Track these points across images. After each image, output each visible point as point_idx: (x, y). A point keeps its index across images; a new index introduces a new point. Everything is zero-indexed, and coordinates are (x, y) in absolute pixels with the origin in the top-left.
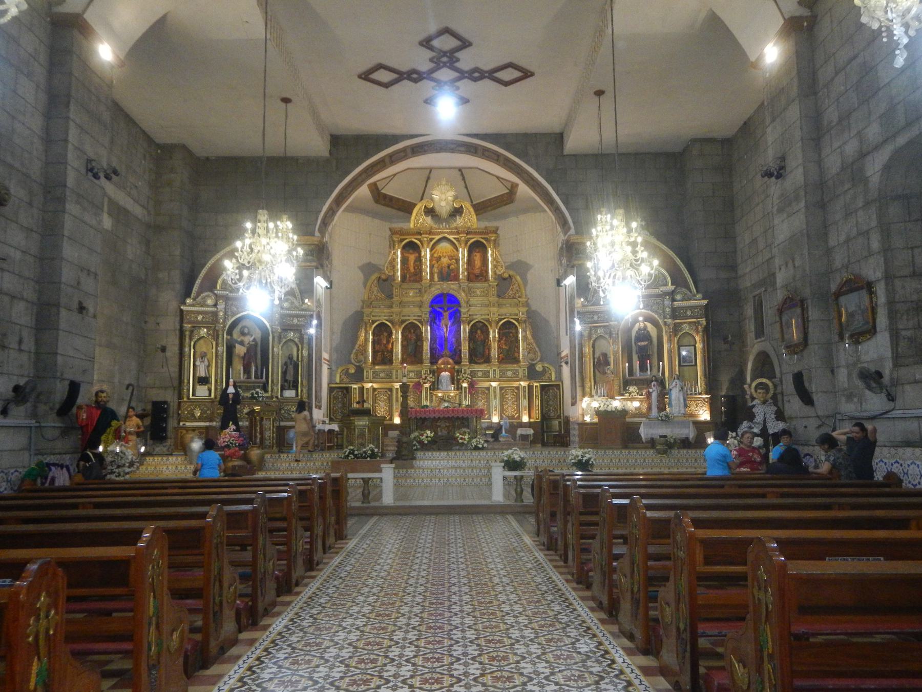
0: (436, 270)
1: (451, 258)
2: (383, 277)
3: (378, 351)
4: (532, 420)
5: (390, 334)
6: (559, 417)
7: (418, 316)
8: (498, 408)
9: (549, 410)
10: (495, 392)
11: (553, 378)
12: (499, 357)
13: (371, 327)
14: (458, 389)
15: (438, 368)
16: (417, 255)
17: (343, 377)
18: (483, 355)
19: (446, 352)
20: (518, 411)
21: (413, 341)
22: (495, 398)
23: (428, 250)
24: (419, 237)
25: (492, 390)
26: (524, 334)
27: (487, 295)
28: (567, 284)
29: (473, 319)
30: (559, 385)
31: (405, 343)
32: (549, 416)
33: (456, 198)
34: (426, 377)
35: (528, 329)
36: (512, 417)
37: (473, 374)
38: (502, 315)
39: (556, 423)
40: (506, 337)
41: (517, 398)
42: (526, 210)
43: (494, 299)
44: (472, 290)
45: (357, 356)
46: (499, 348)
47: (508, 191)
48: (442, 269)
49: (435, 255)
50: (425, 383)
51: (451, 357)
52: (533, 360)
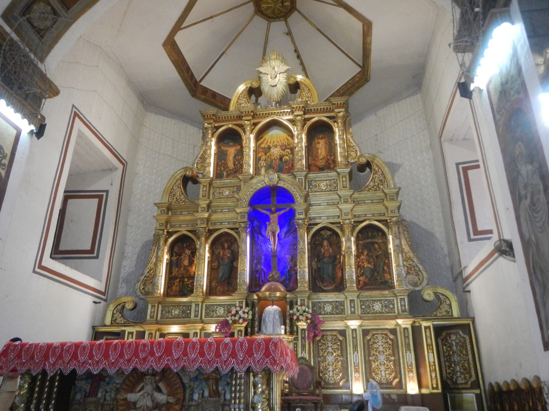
0: (262, 163)
1: (284, 147)
2: (189, 173)
3: (175, 278)
4: (424, 391)
5: (193, 253)
6: (476, 385)
7: (235, 223)
8: (362, 367)
9: (454, 372)
10: (355, 338)
11: (456, 313)
12: (358, 282)
13: (166, 241)
14: (292, 333)
15: (259, 299)
16: (239, 147)
17: (118, 315)
18: (333, 278)
19: (275, 273)
20: (398, 373)
21: (226, 261)
22: (355, 348)
23: (252, 136)
24: (240, 122)
25: (349, 334)
26: (397, 242)
27: (335, 190)
28: (484, 88)
29: (316, 224)
30: (469, 325)
31: (215, 264)
32: (455, 383)
33: (289, 73)
34: (237, 312)
35: (402, 236)
36: (388, 385)
37: (317, 309)
38: (359, 216)
39: (469, 396)
40: (370, 251)
41: (394, 347)
42: (386, 102)
43: (345, 193)
44: (314, 183)
45: (145, 284)
46: (358, 266)
47: (360, 69)
48: (272, 161)
49: (263, 146)
50: (235, 322)
51: (282, 283)
52: (415, 285)
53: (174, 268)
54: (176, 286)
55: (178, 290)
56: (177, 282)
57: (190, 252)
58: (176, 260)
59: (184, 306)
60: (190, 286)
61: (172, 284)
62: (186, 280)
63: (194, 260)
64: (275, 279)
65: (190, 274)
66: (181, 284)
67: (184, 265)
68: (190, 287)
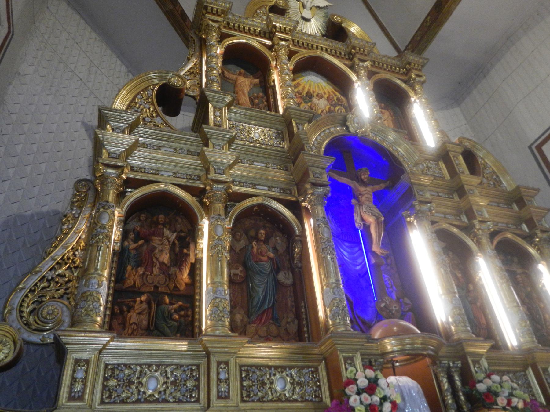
3: (135, 292)
13: (121, 195)
53: (129, 268)
54: (140, 313)
55: (145, 323)
56: (141, 302)
57: (175, 234)
58: (135, 249)
59: (179, 366)
60: (176, 316)
61: (125, 309)
62: (167, 300)
63: (189, 255)
64: (393, 314)
65: (176, 287)
66: (154, 306)
67: (162, 264)
68: (175, 320)
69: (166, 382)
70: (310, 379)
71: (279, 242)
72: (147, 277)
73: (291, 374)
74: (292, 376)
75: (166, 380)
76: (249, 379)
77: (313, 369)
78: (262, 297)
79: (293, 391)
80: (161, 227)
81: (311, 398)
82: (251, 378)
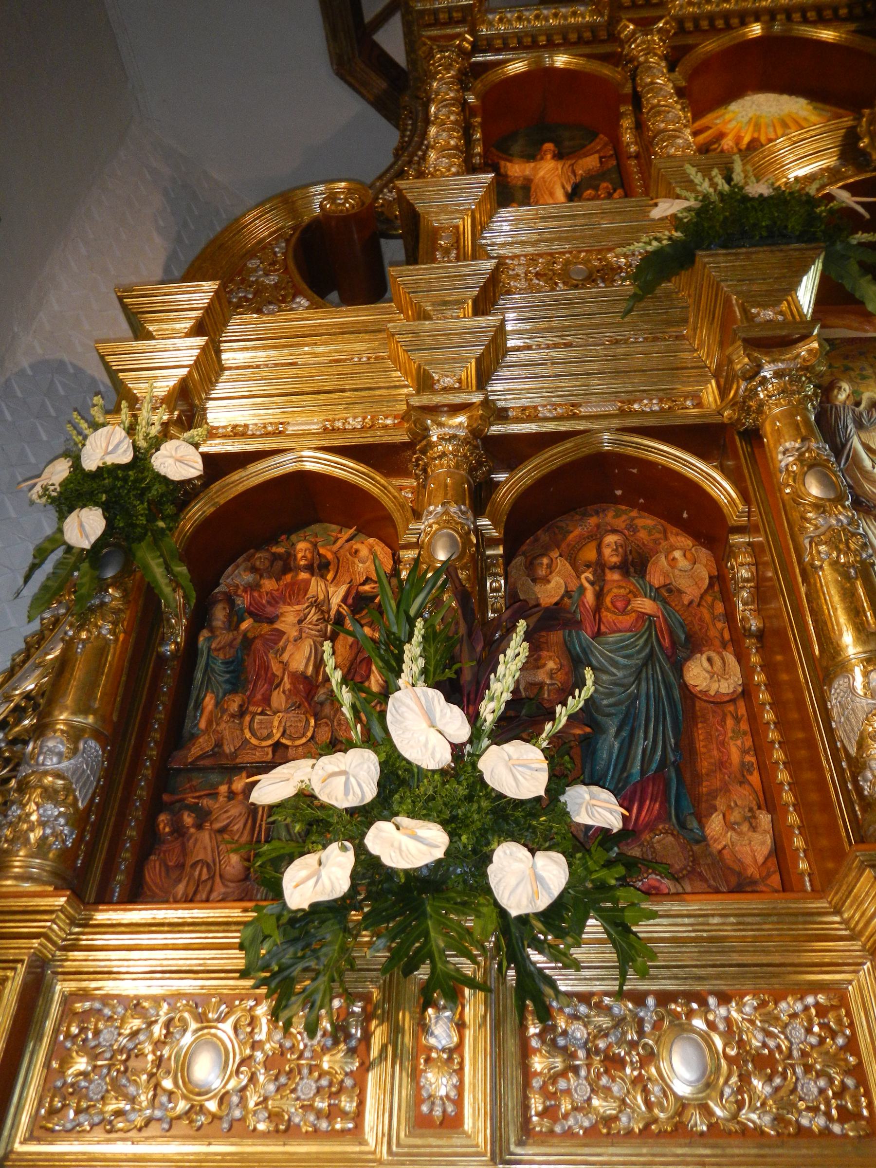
53: (209, 702)
61: (188, 819)
69: (250, 1057)
70: (813, 1040)
71: (683, 563)
72: (252, 720)
73: (728, 1020)
74: (730, 1032)
75: (248, 1052)
76: (554, 1041)
77: (821, 998)
78: (617, 745)
79: (739, 1091)
80: (303, 575)
81: (821, 1121)
82: (561, 1042)
